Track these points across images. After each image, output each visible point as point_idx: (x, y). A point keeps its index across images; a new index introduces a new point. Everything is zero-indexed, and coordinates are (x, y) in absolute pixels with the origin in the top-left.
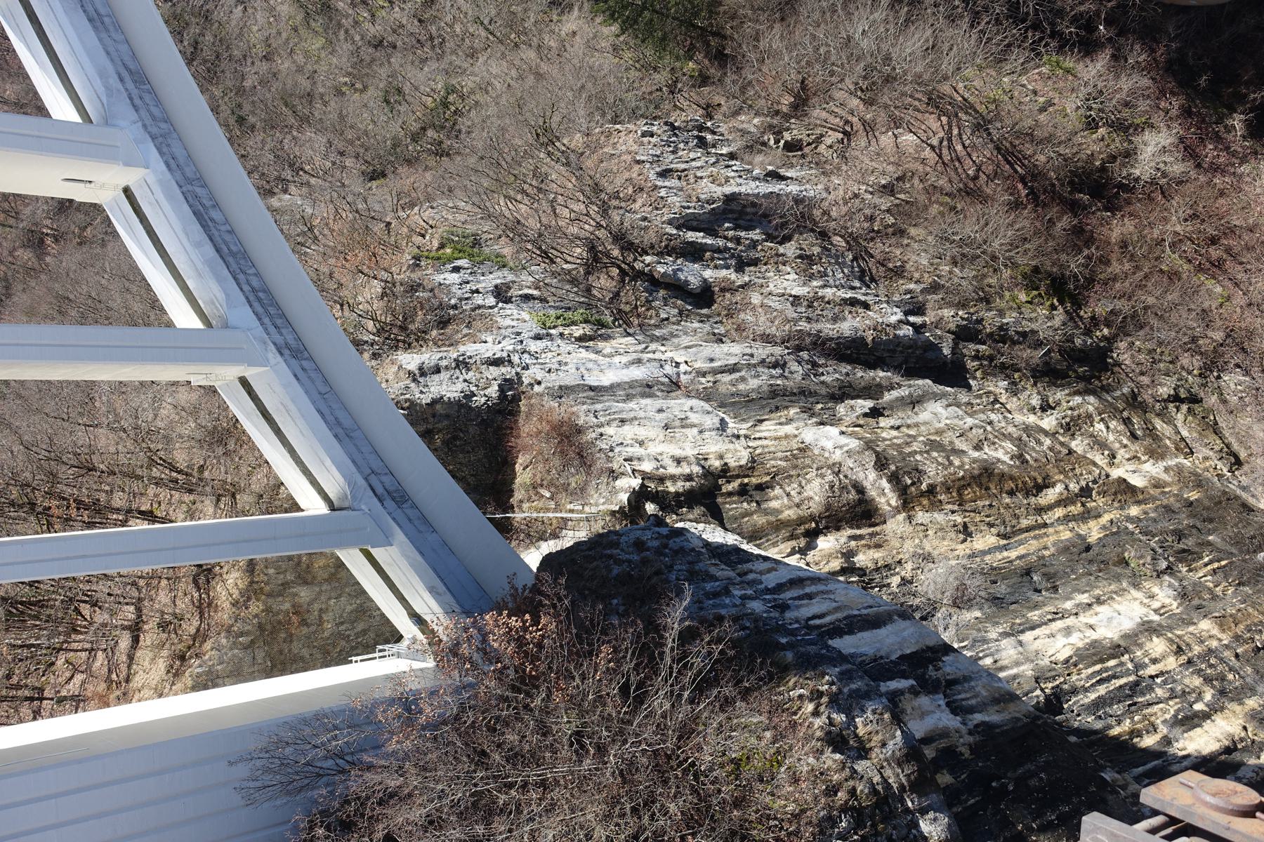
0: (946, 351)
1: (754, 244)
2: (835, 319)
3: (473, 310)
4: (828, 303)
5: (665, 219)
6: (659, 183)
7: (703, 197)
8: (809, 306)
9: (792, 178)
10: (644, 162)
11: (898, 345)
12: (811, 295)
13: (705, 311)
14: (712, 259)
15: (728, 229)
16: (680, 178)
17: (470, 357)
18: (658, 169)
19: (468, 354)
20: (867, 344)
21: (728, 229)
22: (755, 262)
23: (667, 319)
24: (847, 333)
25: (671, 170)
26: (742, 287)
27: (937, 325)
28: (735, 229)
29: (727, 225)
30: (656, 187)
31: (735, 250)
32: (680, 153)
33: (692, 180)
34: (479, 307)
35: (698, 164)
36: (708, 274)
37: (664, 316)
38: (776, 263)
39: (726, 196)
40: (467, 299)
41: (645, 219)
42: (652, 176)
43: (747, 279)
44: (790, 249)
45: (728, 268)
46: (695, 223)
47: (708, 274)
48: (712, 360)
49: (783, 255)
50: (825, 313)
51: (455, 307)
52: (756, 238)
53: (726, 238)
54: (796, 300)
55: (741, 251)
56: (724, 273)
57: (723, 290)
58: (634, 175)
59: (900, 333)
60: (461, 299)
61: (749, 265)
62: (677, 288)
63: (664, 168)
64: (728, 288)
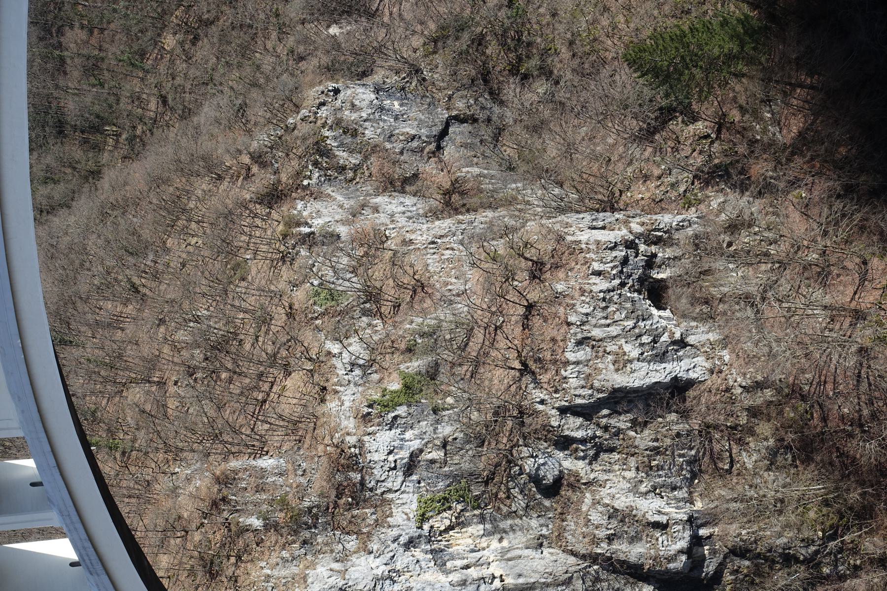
0: (710, 567)
1: (619, 432)
2: (633, 540)
3: (383, 493)
4: (637, 521)
5: (557, 405)
6: (570, 356)
7: (597, 384)
8: (622, 521)
9: (692, 346)
10: (572, 324)
11: (667, 573)
12: (627, 511)
13: (547, 503)
14: (576, 450)
15: (604, 416)
16: (593, 347)
17: (350, 587)
18: (579, 336)
19: (350, 583)
20: (644, 569)
21: (604, 416)
22: (611, 450)
23: (515, 512)
24: (633, 559)
25: (589, 338)
26: (585, 484)
27: (721, 538)
28: (609, 416)
29: (605, 412)
30: (567, 363)
31: (600, 437)
32: (612, 308)
33: (600, 354)
34: (390, 491)
35: (614, 330)
36: (568, 464)
37: (514, 509)
38: (627, 454)
39: (614, 389)
40: (383, 481)
41: (542, 402)
42: (571, 345)
43: (592, 476)
44: (644, 439)
45: (584, 458)
46: (579, 409)
47: (568, 464)
48: (520, 575)
49: (636, 447)
50: (629, 530)
51: (371, 490)
52: (622, 426)
53: (598, 425)
54: (613, 514)
55: (606, 440)
56: (581, 464)
57: (571, 486)
58: (559, 338)
59: (672, 566)
60: (378, 481)
61: (606, 451)
62: (536, 479)
63: (586, 334)
64: (576, 483)
